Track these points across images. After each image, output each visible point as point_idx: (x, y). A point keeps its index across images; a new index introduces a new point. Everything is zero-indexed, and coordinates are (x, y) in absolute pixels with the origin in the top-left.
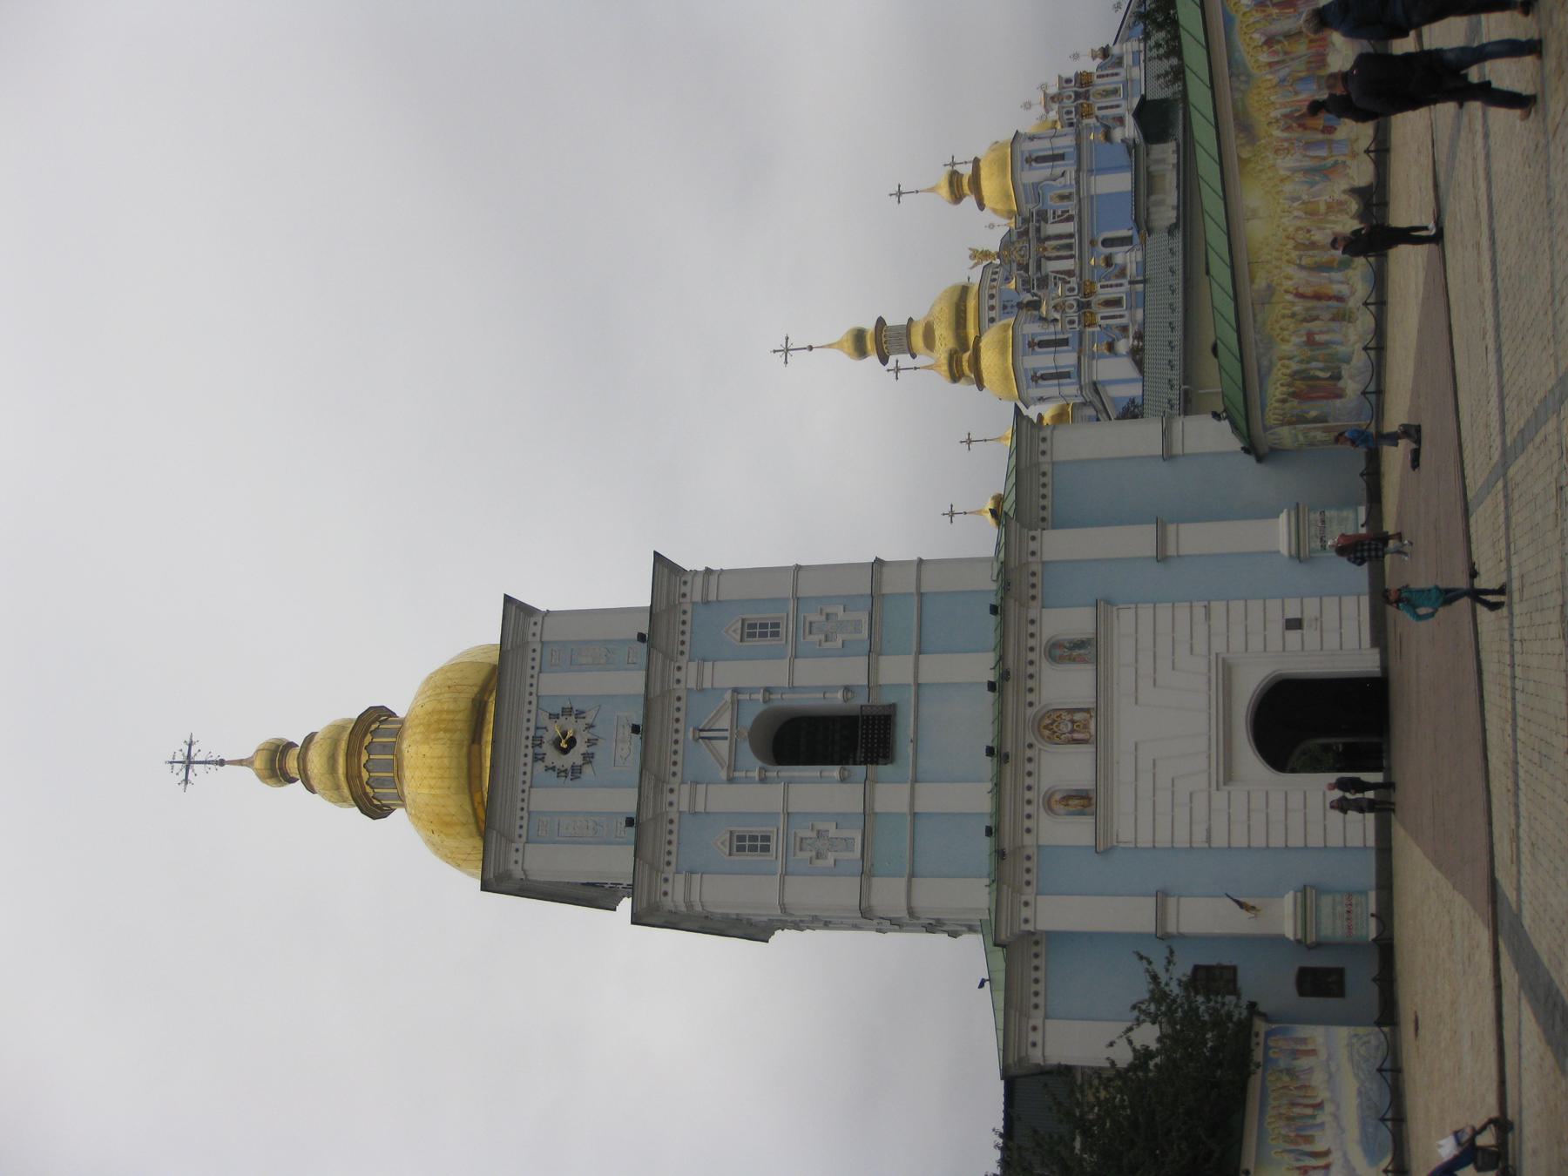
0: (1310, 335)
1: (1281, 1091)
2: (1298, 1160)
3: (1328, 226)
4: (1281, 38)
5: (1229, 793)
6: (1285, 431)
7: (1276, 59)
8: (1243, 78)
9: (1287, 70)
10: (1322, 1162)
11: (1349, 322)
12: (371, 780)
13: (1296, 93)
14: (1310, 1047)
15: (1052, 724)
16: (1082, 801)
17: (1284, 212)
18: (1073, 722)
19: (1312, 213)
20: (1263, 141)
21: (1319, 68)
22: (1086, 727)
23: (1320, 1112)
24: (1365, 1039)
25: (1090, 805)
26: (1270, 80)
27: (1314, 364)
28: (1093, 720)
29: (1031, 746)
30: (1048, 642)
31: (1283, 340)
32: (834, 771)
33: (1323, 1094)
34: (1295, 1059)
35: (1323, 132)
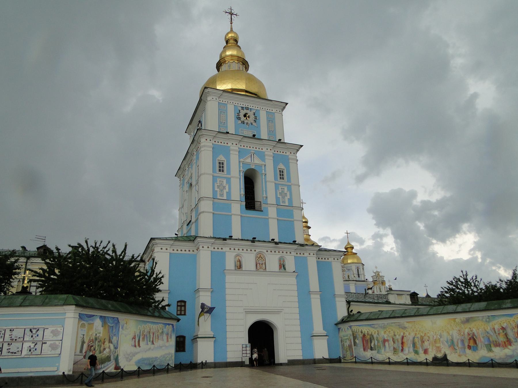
0: (388, 340)
1: (157, 329)
2: (137, 335)
3: (431, 348)
4: (505, 332)
5: (243, 313)
6: (350, 332)
7: (496, 331)
8: (488, 320)
9: (492, 334)
11: (393, 353)
12: (230, 63)
13: (483, 337)
14: (169, 339)
15: (261, 258)
16: (239, 266)
17: (435, 332)
18: (262, 264)
19: (435, 342)
20: (463, 326)
21: (494, 345)
22: (261, 268)
23: (151, 343)
25: (238, 268)
26: (488, 329)
27: (376, 342)
28: (263, 270)
29: (255, 251)
30: (285, 258)
31: (385, 332)
32: (243, 192)
33: (157, 344)
35: (468, 346)
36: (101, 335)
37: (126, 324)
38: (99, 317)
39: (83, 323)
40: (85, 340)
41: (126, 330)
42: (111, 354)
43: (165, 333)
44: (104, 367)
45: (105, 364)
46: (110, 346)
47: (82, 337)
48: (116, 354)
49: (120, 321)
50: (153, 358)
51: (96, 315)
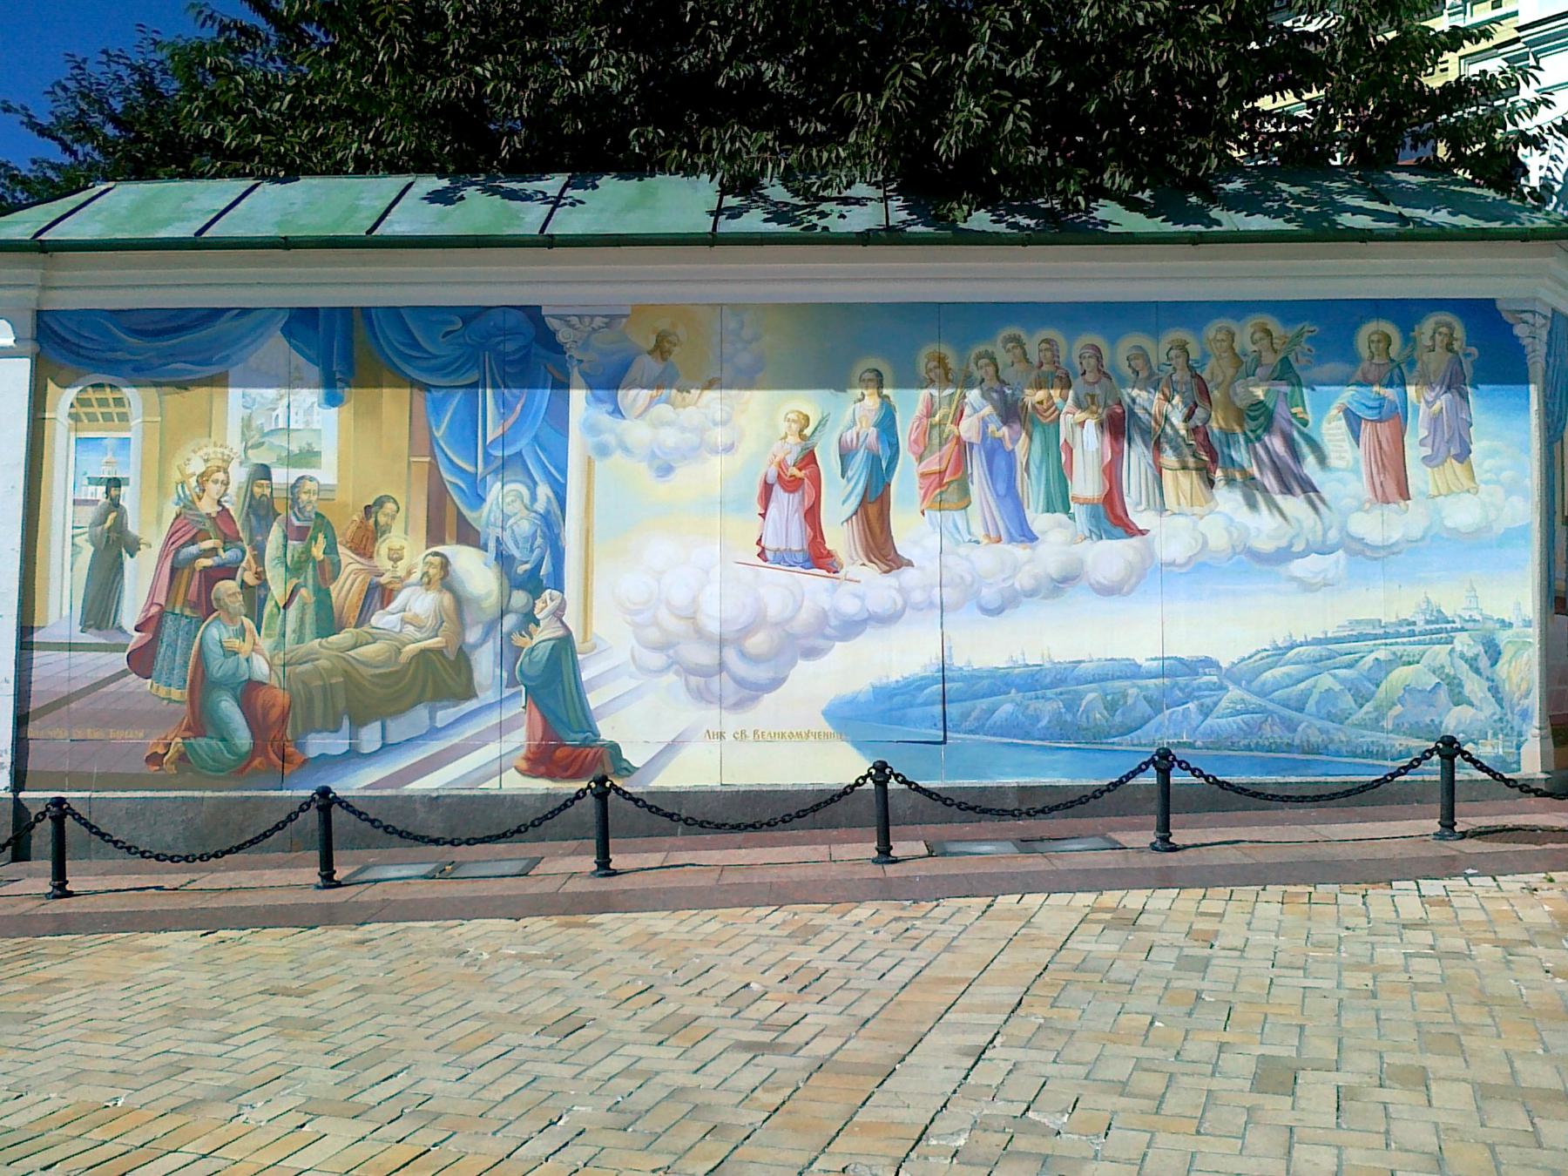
2: (846, 455)
10: (840, 535)
24: (1474, 687)
36: (326, 474)
38: (282, 320)
40: (133, 527)
42: (472, 636)
44: (386, 747)
45: (392, 725)
46: (445, 564)
47: (95, 502)
48: (546, 633)
49: (562, 336)
50: (1132, 672)
51: (245, 311)
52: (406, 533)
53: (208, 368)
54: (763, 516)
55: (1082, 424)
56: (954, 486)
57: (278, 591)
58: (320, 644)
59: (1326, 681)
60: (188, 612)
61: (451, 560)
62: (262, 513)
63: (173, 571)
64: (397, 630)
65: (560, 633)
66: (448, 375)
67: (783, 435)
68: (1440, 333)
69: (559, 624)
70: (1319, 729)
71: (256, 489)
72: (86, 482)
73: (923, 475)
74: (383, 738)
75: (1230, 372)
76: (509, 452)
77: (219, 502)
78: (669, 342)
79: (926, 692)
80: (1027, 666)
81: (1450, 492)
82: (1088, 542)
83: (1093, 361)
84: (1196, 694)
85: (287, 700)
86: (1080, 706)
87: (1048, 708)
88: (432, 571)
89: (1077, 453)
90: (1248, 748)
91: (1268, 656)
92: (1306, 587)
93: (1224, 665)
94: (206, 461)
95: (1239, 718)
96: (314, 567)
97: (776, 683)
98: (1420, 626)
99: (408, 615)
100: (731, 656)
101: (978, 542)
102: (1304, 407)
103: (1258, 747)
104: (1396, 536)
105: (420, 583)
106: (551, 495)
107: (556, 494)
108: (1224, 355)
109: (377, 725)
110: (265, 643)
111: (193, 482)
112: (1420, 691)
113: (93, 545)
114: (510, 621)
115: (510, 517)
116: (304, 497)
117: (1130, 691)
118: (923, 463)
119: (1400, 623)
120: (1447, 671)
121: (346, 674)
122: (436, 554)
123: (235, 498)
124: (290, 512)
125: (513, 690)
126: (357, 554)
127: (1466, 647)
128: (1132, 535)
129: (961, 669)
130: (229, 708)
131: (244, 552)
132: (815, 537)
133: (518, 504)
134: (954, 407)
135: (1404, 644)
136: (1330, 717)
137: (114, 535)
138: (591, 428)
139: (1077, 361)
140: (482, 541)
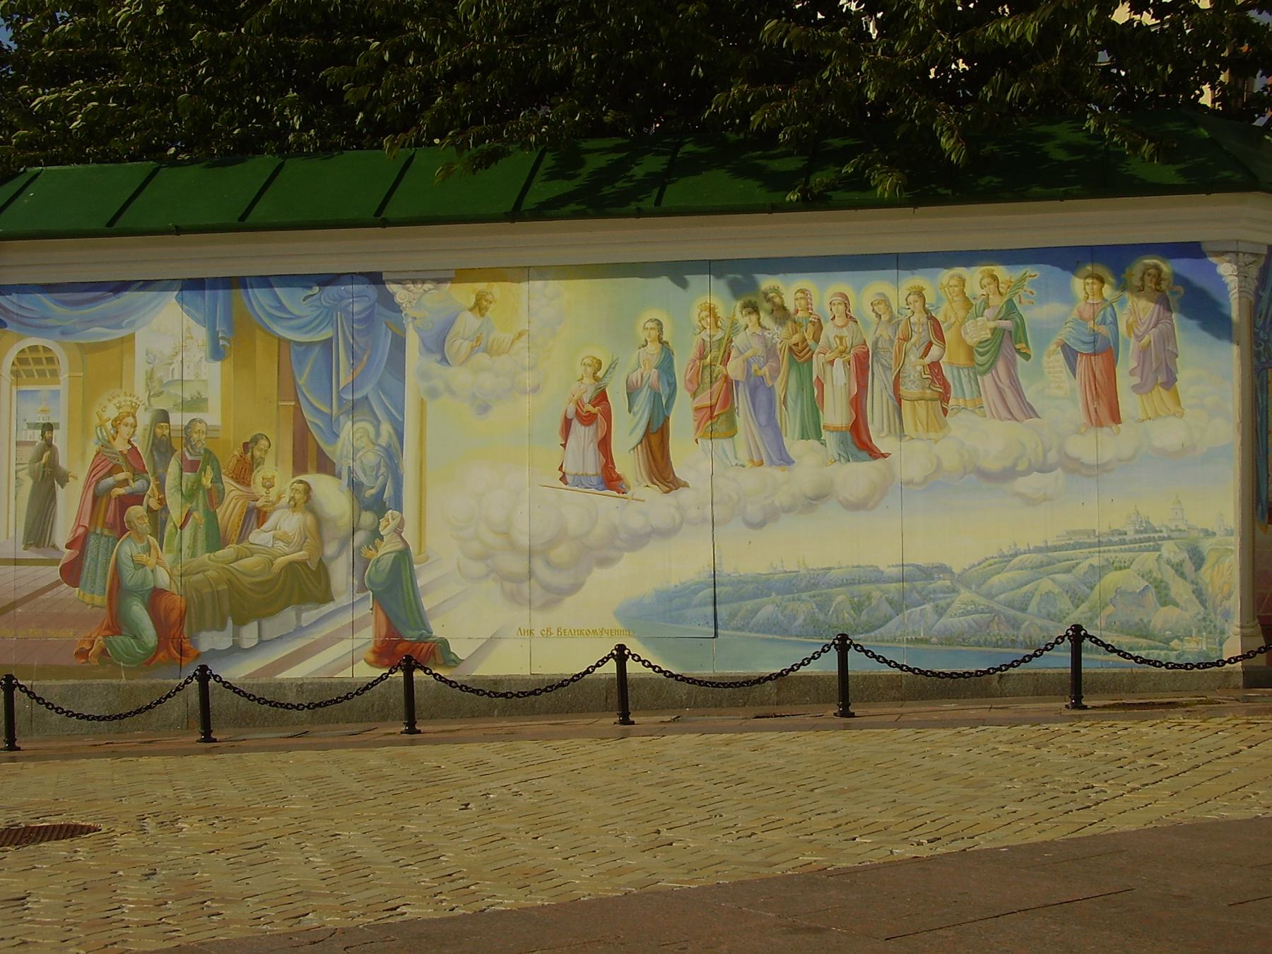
1: (918, 318)
2: (632, 393)
10: (627, 461)
14: (1128, 402)
24: (1180, 589)
34: (1070, 355)
36: (212, 417)
37: (479, 307)
39: (34, 349)
40: (63, 462)
41: (481, 358)
42: (330, 550)
43: (1053, 347)
44: (262, 643)
45: (266, 624)
46: (308, 490)
48: (388, 547)
50: (877, 578)
52: (276, 465)
53: (120, 331)
54: (564, 446)
55: (832, 363)
56: (723, 418)
57: (175, 514)
58: (209, 557)
59: (1046, 584)
60: (106, 532)
61: (312, 487)
62: (163, 450)
63: (96, 499)
64: (270, 546)
65: (400, 546)
66: (306, 333)
67: (580, 377)
68: (1149, 275)
69: (399, 540)
70: (1041, 628)
71: (158, 431)
72: (25, 427)
73: (697, 409)
74: (260, 636)
75: (961, 313)
76: (358, 396)
77: (129, 442)
78: (486, 301)
79: (701, 594)
80: (786, 572)
81: (1158, 416)
82: (838, 462)
83: (842, 308)
84: (932, 596)
85: (183, 605)
86: (830, 607)
87: (803, 609)
88: (297, 496)
89: (827, 388)
90: (978, 644)
91: (995, 563)
92: (1030, 501)
93: (956, 570)
94: (119, 408)
95: (969, 618)
96: (204, 491)
97: (575, 588)
98: (1131, 535)
99: (279, 533)
100: (539, 565)
101: (743, 466)
102: (1026, 342)
103: (986, 643)
104: (1108, 454)
105: (288, 506)
106: (392, 431)
107: (395, 429)
108: (955, 299)
109: (256, 623)
110: (167, 558)
111: (109, 425)
112: (1130, 593)
113: (33, 478)
114: (360, 537)
115: (359, 450)
116: (195, 436)
117: (874, 594)
118: (697, 399)
119: (1113, 533)
120: (1155, 575)
121: (230, 582)
122: (301, 482)
123: (141, 438)
124: (185, 449)
125: (362, 595)
126: (238, 483)
127: (1172, 554)
128: (876, 458)
129: (729, 575)
130: (139, 612)
131: (149, 483)
132: (606, 466)
133: (364, 439)
134: (722, 351)
135: (1115, 551)
136: (1049, 616)
137: (48, 470)
138: (424, 375)
139: (828, 307)
140: (337, 471)
